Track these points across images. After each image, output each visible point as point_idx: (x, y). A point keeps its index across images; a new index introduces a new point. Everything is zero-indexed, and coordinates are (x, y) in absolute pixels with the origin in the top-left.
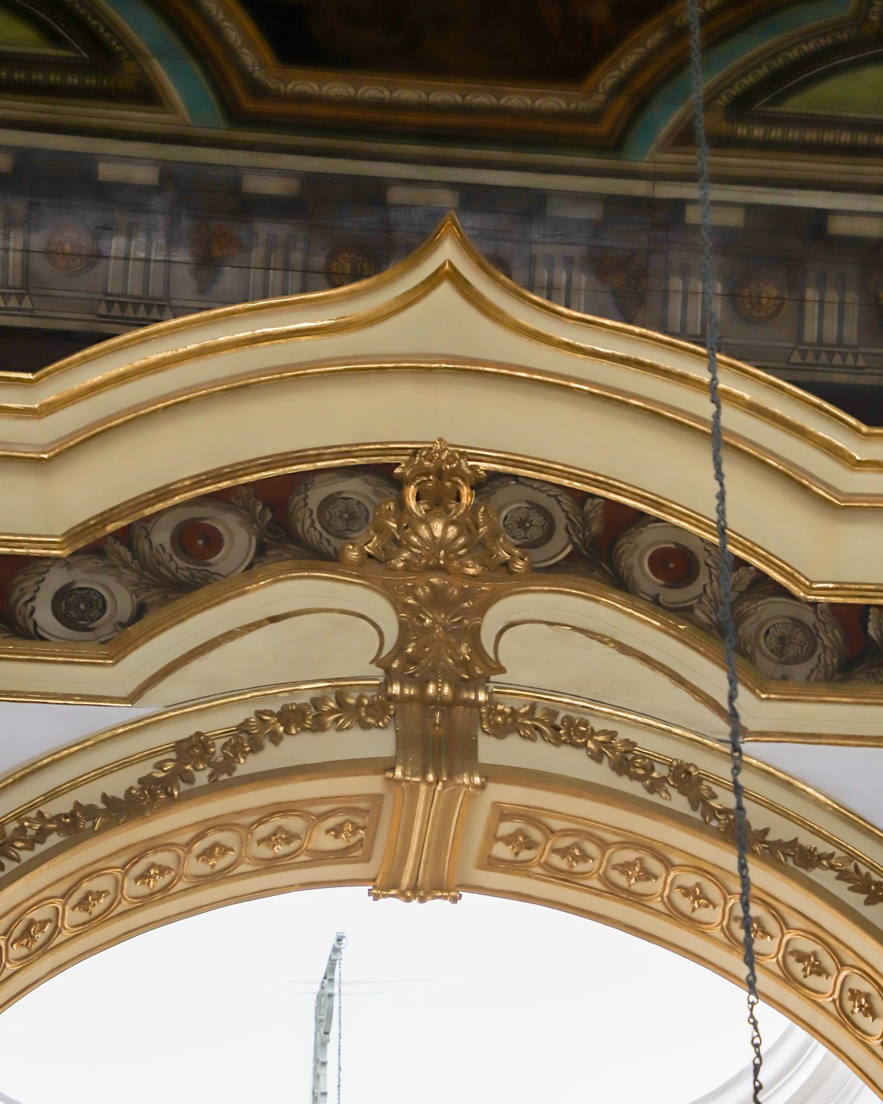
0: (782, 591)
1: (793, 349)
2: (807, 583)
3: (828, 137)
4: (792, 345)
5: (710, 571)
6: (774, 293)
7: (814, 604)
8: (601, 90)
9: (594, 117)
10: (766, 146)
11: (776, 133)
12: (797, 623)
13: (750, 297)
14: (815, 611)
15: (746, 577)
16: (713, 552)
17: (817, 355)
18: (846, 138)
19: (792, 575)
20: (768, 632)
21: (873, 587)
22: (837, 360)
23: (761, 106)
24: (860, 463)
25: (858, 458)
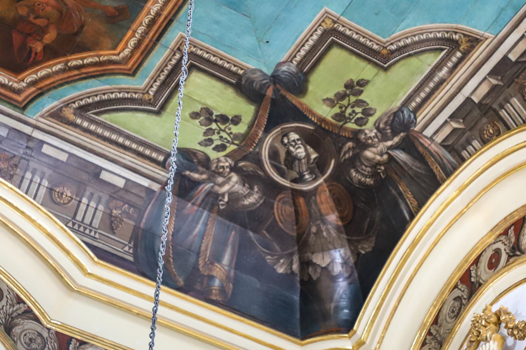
0: (37, 320)
1: (70, 221)
2: (49, 319)
3: (114, 137)
4: (70, 219)
5: (7, 301)
6: (69, 194)
7: (49, 329)
8: (25, 81)
9: (18, 92)
10: (86, 131)
11: (93, 127)
12: (40, 335)
13: (59, 192)
14: (49, 333)
15: (23, 308)
16: (11, 293)
17: (79, 226)
18: (121, 140)
19: (43, 314)
20: (25, 335)
21: (77, 330)
22: (87, 232)
23: (91, 113)
24: (90, 274)
25: (89, 272)
